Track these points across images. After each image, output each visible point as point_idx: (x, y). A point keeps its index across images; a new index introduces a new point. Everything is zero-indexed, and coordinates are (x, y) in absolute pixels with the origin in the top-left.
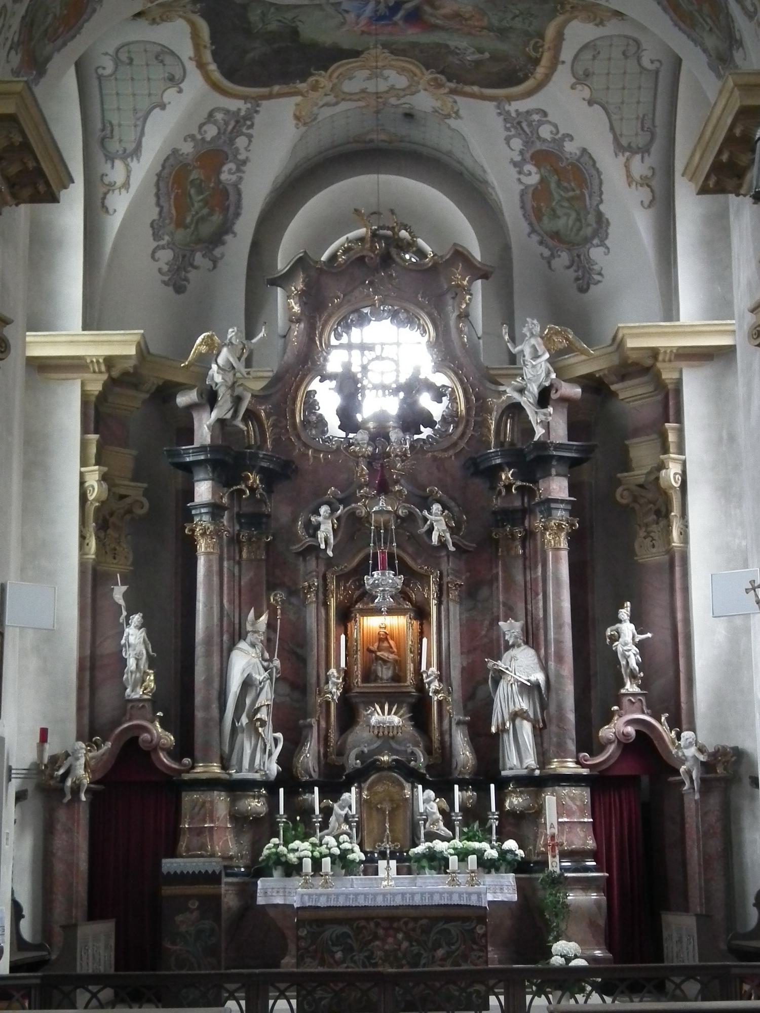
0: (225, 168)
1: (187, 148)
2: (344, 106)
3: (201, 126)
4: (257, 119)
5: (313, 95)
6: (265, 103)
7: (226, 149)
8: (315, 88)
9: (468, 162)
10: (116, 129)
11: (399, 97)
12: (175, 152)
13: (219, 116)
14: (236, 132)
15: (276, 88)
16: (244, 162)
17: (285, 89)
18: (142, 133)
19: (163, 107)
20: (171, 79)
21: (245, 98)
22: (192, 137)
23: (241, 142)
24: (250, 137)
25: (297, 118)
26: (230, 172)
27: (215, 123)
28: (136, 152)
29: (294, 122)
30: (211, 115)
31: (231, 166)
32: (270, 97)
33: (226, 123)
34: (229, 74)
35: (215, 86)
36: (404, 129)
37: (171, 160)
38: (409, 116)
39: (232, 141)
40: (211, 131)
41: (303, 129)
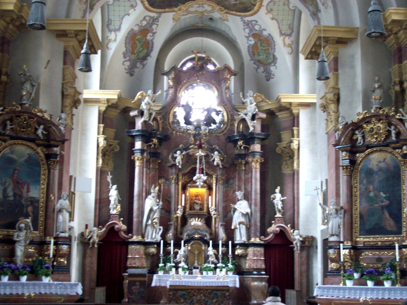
0: (149, 35)
1: (136, 28)
2: (189, 15)
3: (141, 21)
4: (160, 19)
5: (179, 12)
6: (163, 14)
7: (149, 29)
8: (180, 10)
9: (230, 35)
10: (113, 21)
11: (207, 13)
12: (132, 30)
13: (147, 18)
14: (153, 23)
15: (167, 10)
16: (155, 33)
17: (170, 10)
18: (121, 23)
19: (129, 15)
20: (132, 6)
21: (156, 12)
22: (138, 25)
23: (154, 27)
24: (157, 25)
25: (174, 19)
26: (150, 36)
27: (146, 20)
28: (119, 29)
29: (172, 20)
30: (144, 18)
31: (150, 34)
32: (165, 12)
33: (150, 20)
34: (152, 5)
35: (147, 9)
36: (209, 23)
37: (131, 33)
38: (211, 19)
39: (151, 26)
40: (144, 23)
41: (175, 23)
